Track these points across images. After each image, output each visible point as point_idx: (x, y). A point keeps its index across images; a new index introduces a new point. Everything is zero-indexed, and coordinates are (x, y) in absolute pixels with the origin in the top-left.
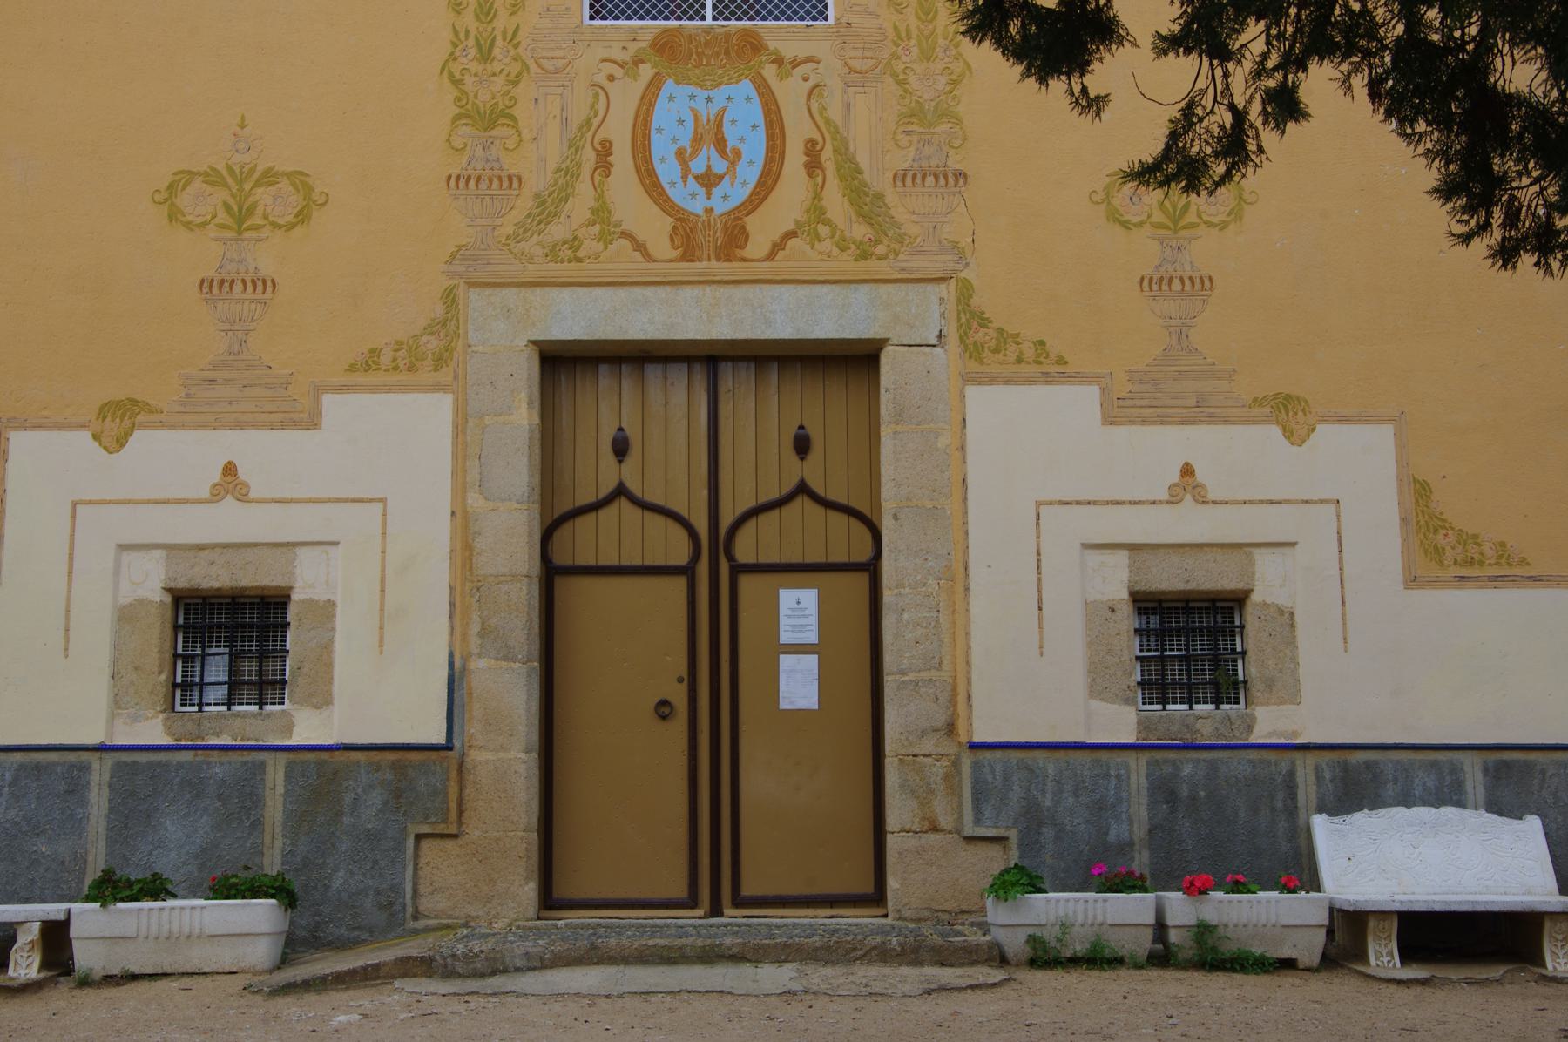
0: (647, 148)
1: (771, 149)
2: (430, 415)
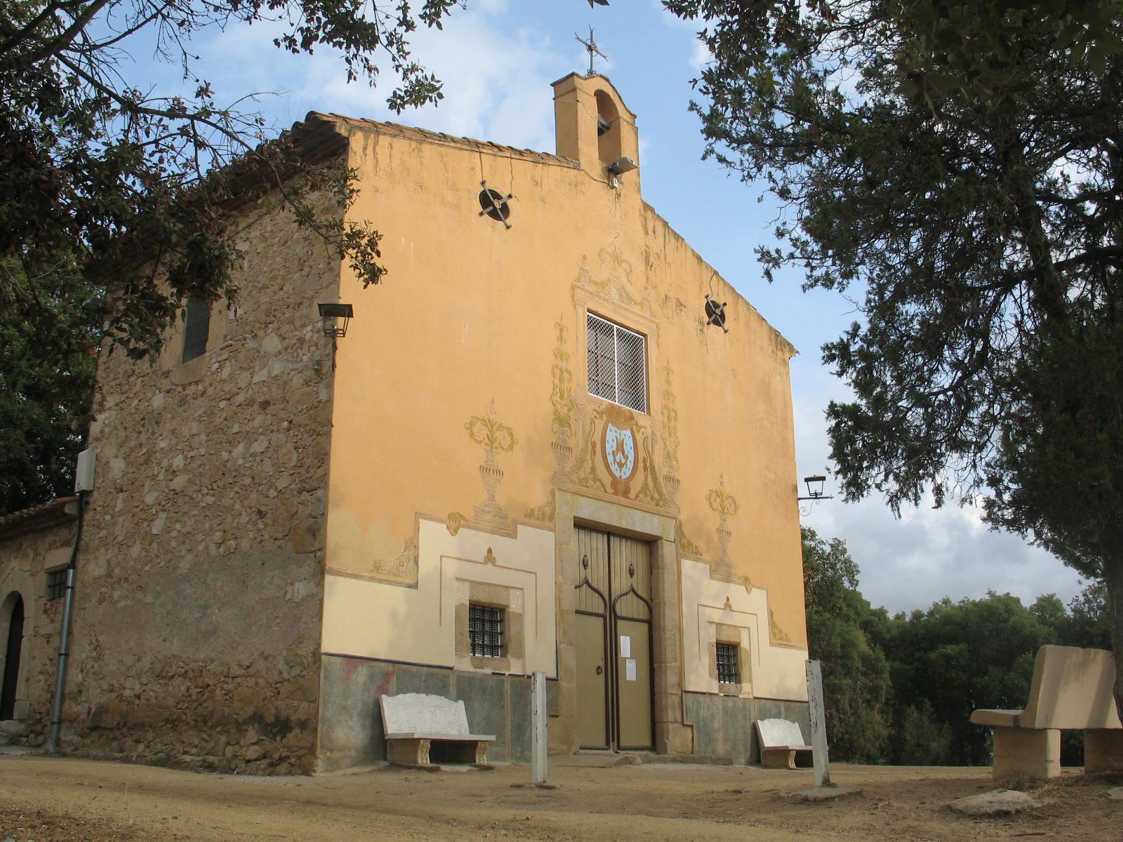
2: (548, 538)
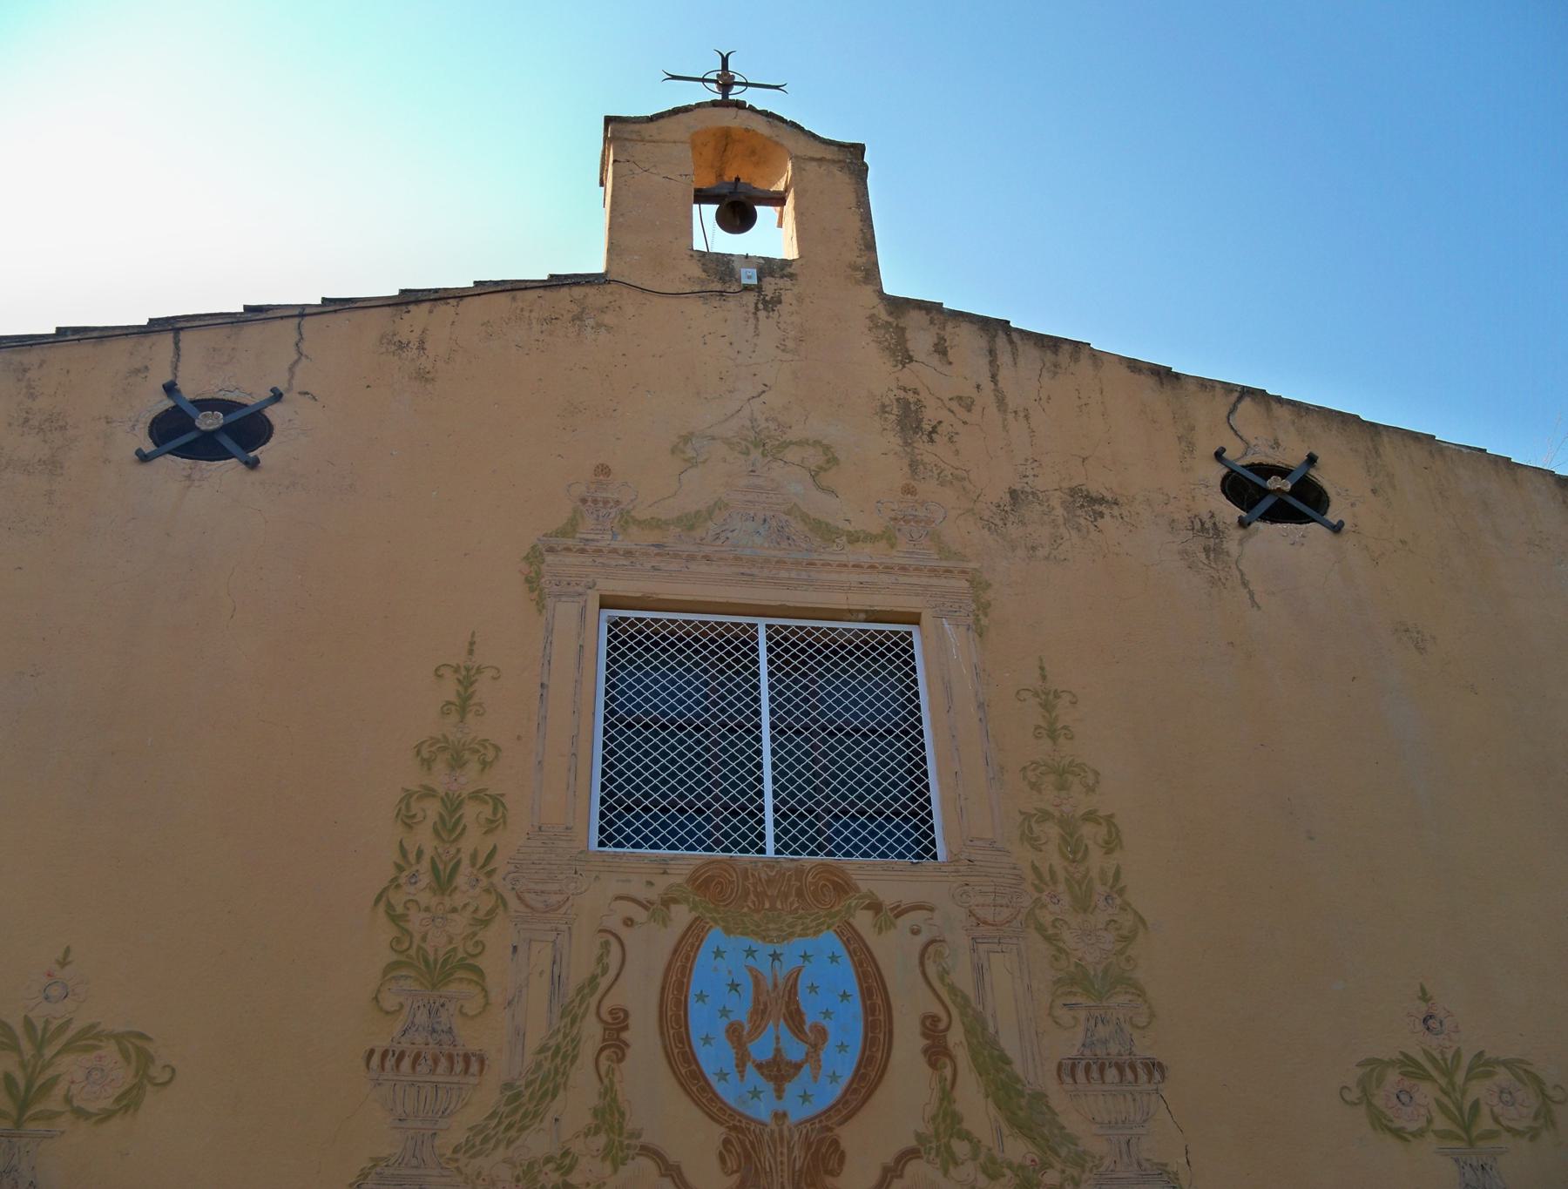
0: (683, 1022)
1: (870, 1026)
